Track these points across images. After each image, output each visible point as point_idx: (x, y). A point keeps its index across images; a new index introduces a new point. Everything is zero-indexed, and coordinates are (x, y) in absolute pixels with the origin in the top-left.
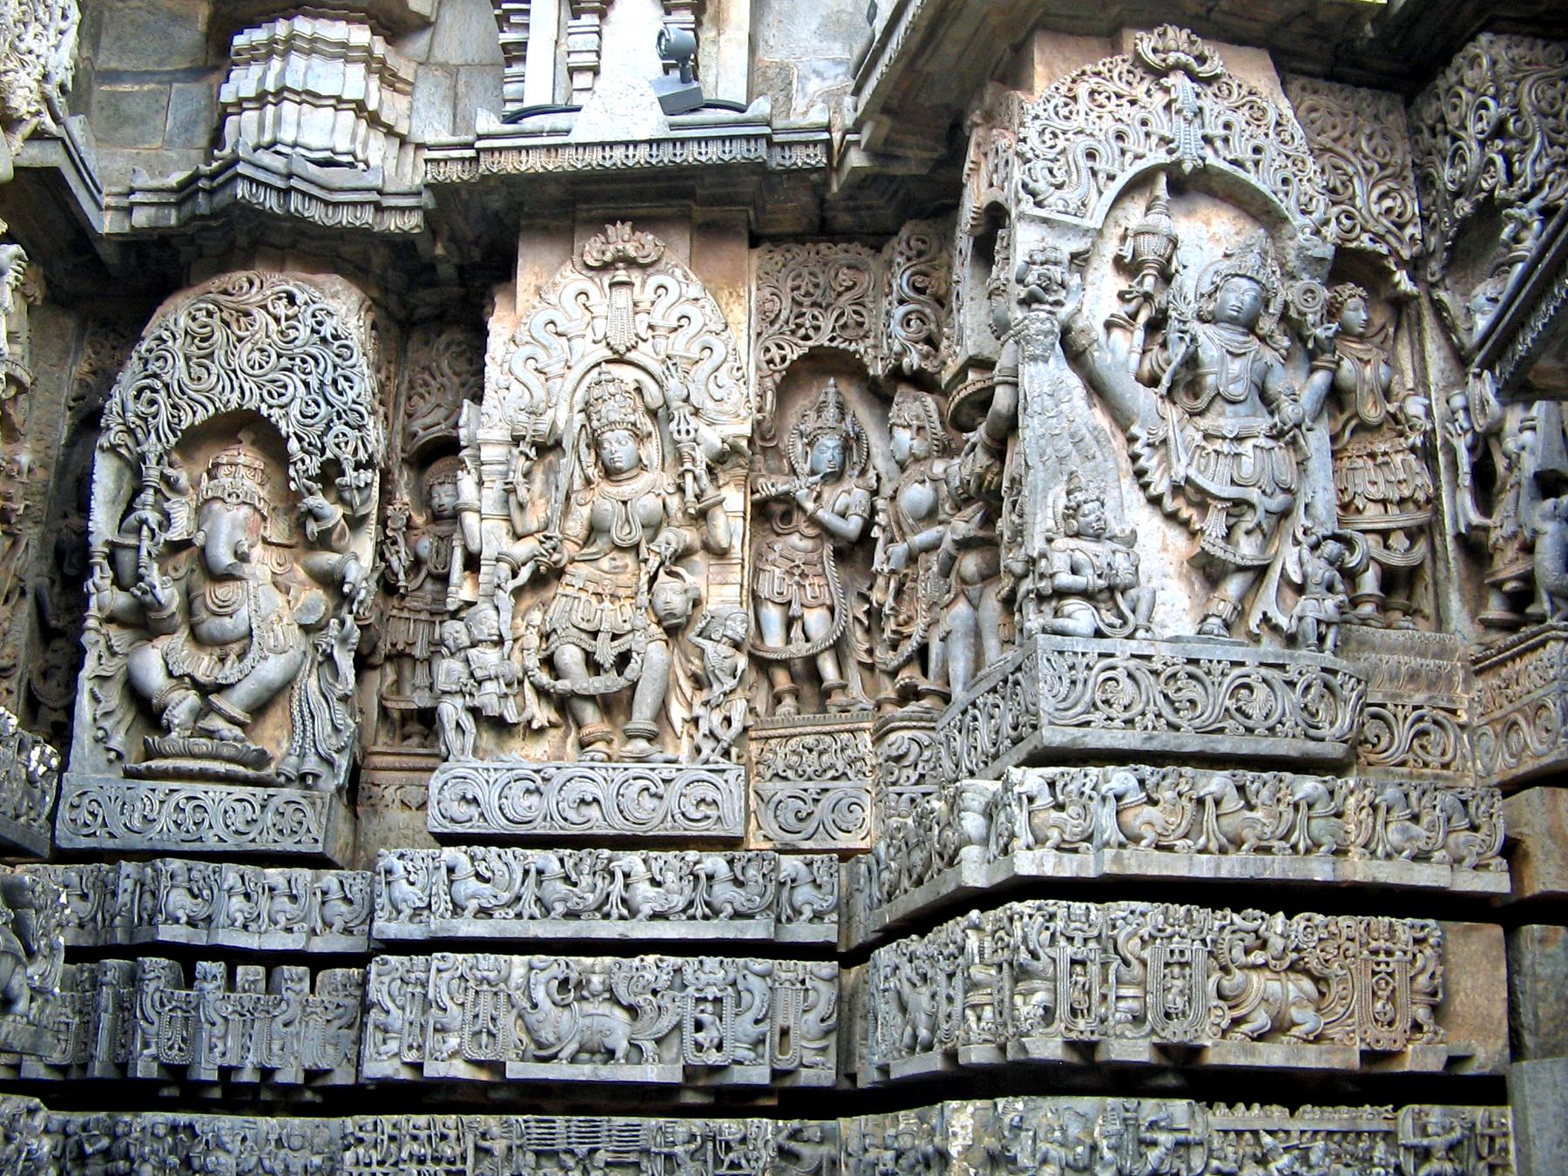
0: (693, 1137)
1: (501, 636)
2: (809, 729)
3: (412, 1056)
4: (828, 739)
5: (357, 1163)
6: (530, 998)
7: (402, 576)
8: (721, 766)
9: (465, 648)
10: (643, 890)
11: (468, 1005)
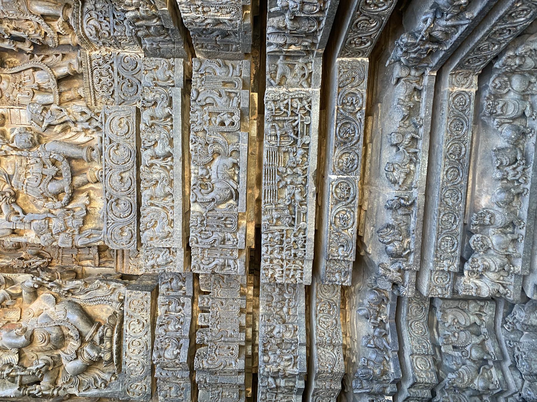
0: (273, 127)
1: (45, 219)
2: (91, 81)
3: (236, 254)
4: (95, 72)
5: (282, 276)
6: (210, 202)
7: (44, 260)
8: (103, 116)
9: (52, 235)
10: (159, 150)
11: (213, 229)
